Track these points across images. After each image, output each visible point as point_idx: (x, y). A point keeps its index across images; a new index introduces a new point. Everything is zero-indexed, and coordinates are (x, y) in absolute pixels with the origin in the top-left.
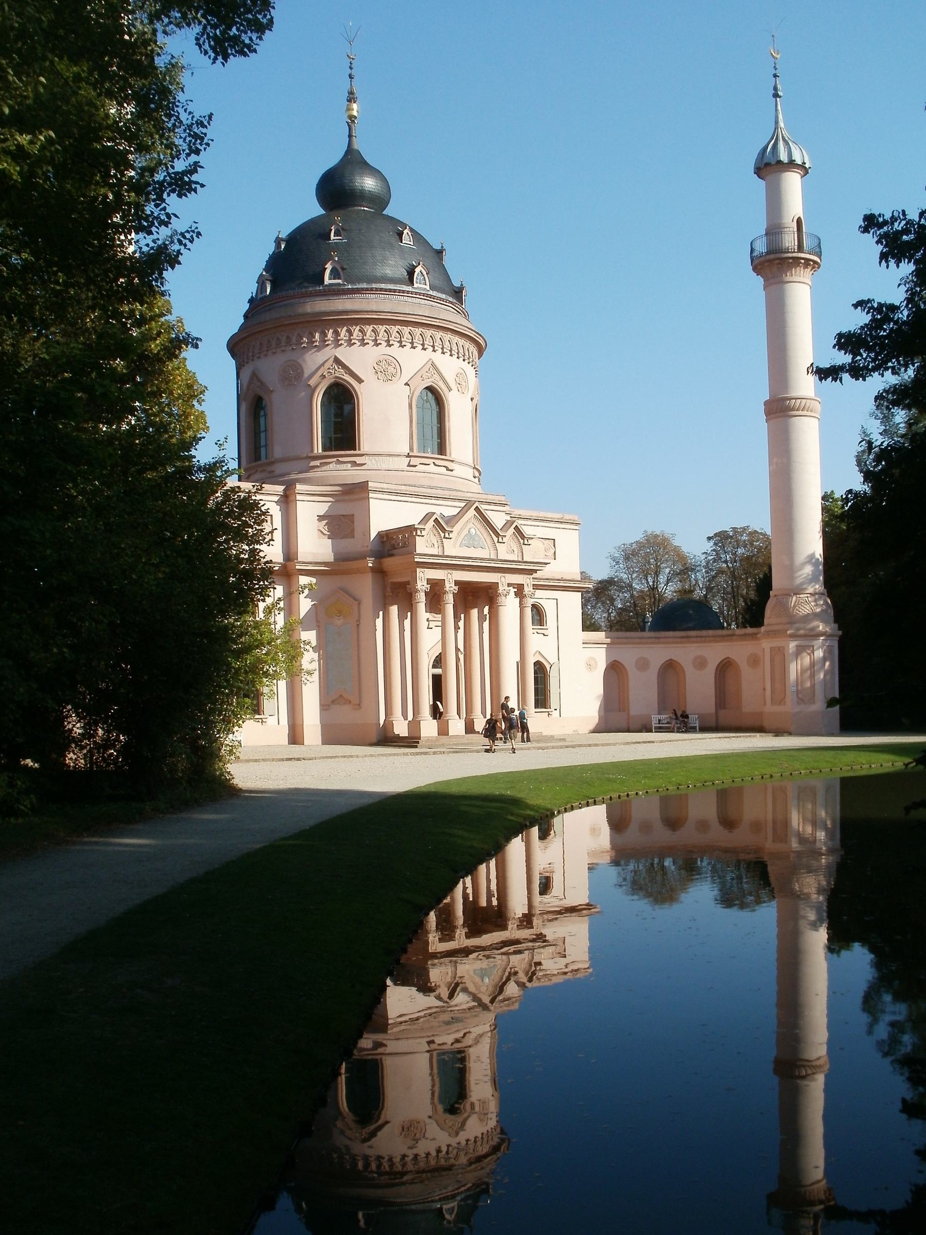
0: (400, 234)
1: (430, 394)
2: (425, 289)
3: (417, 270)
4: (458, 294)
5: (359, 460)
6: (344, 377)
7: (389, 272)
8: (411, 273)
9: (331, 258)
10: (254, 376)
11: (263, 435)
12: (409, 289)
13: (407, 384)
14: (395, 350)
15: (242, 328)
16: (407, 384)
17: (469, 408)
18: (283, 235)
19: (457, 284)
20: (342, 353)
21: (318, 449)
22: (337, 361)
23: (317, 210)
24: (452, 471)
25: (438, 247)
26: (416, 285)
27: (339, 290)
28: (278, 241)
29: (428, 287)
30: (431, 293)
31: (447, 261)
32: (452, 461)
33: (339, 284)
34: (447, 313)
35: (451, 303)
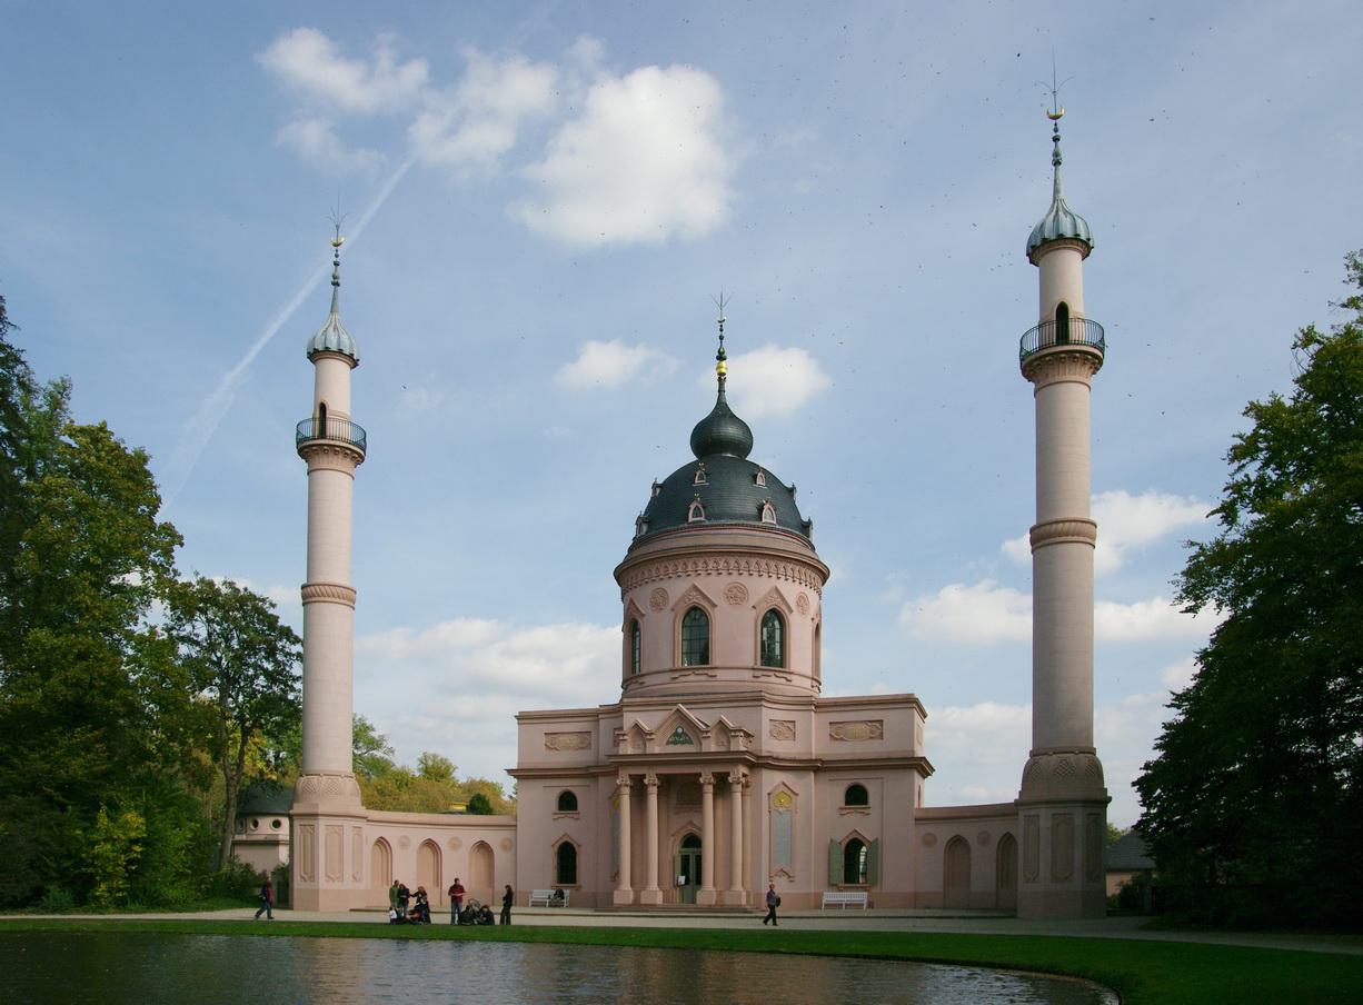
0: (755, 477)
3: (766, 507)
4: (805, 527)
5: (711, 673)
7: (739, 510)
8: (761, 509)
9: (693, 499)
11: (637, 652)
12: (756, 523)
13: (754, 607)
14: (744, 579)
15: (624, 562)
16: (754, 607)
17: (810, 628)
18: (660, 482)
19: (805, 519)
20: (701, 582)
22: (695, 587)
23: (690, 457)
28: (655, 486)
31: (799, 499)
33: (701, 521)
34: (792, 545)
35: (797, 535)
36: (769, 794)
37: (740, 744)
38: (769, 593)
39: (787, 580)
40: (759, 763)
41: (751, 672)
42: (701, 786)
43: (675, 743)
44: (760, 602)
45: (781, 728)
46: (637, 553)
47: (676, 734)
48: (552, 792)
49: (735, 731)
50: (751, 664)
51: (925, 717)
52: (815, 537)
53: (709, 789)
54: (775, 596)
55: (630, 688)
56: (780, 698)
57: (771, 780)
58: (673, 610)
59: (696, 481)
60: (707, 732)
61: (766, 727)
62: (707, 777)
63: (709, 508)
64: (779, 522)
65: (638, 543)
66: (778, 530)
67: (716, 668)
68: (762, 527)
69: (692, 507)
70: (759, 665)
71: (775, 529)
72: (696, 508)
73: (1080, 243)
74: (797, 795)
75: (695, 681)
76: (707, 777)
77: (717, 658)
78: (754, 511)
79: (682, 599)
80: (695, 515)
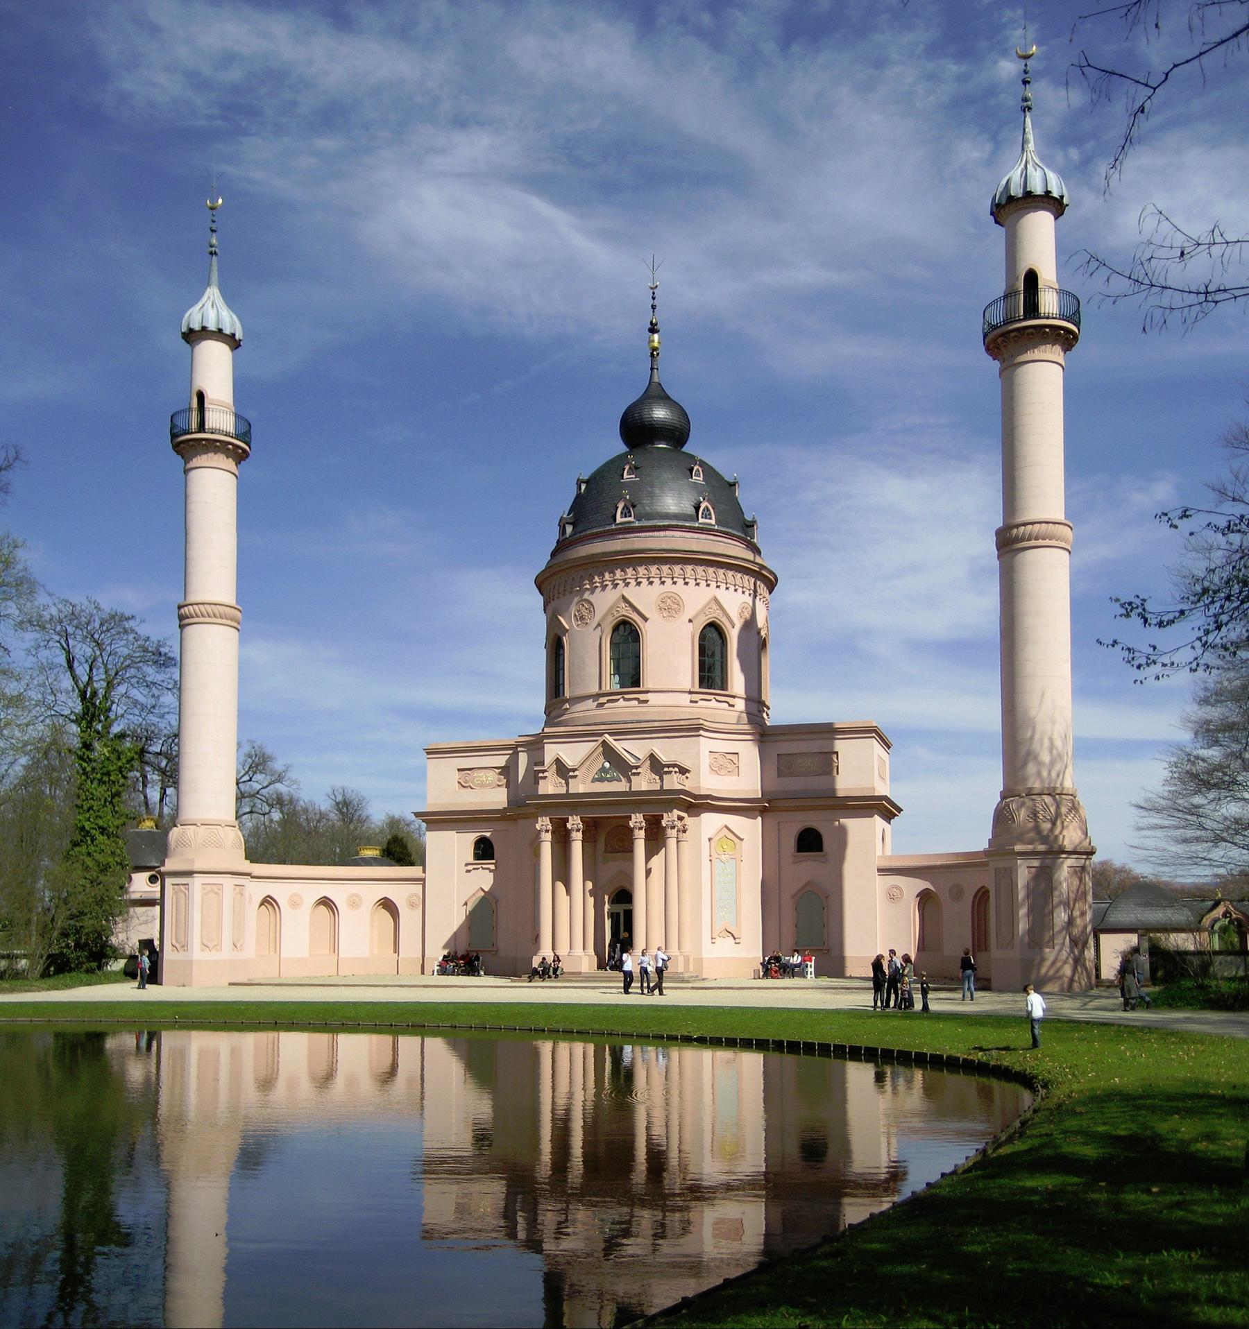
0: (691, 470)
1: (713, 630)
2: (711, 525)
5: (642, 697)
6: (631, 616)
8: (697, 508)
9: (622, 497)
13: (690, 621)
14: (679, 587)
16: (690, 621)
19: (748, 517)
20: (631, 593)
24: (733, 706)
25: (731, 481)
26: (701, 520)
27: (629, 528)
28: (579, 482)
29: (713, 522)
30: (716, 527)
32: (734, 697)
34: (736, 550)
36: (710, 840)
37: (673, 782)
38: (710, 601)
39: (727, 588)
40: (697, 805)
41: (688, 697)
42: (631, 830)
43: (601, 780)
44: (696, 616)
45: (722, 761)
46: (559, 558)
47: (603, 769)
48: (471, 837)
49: (668, 766)
50: (688, 687)
51: (889, 747)
53: (640, 836)
54: (715, 607)
55: (553, 714)
56: (721, 726)
57: (711, 822)
58: (599, 625)
59: (625, 476)
60: (637, 767)
61: (705, 760)
62: (637, 820)
63: (639, 507)
64: (718, 522)
65: (562, 545)
66: (717, 531)
67: (647, 692)
68: (698, 528)
69: (621, 506)
70: (697, 688)
71: (714, 530)
72: (625, 507)
73: (1052, 202)
74: (741, 840)
75: (624, 709)
76: (637, 820)
77: (648, 681)
78: (692, 511)
79: (609, 612)
80: (624, 515)
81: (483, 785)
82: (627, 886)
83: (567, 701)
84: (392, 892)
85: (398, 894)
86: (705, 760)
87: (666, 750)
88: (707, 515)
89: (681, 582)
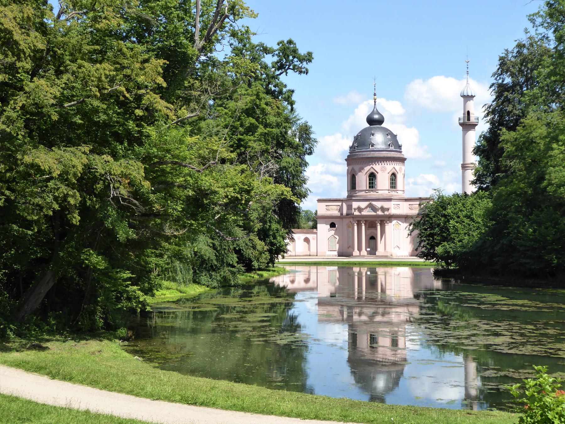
8: (389, 145)
10: (353, 169)
21: (368, 188)
22: (372, 168)
37: (386, 213)
40: (391, 218)
41: (387, 192)
45: (396, 206)
52: (403, 149)
57: (394, 222)
61: (393, 206)
75: (372, 195)
81: (332, 209)
82: (374, 236)
83: (357, 191)
84: (309, 236)
85: (310, 236)
86: (393, 206)
87: (386, 204)
88: (392, 147)
89: (386, 164)
